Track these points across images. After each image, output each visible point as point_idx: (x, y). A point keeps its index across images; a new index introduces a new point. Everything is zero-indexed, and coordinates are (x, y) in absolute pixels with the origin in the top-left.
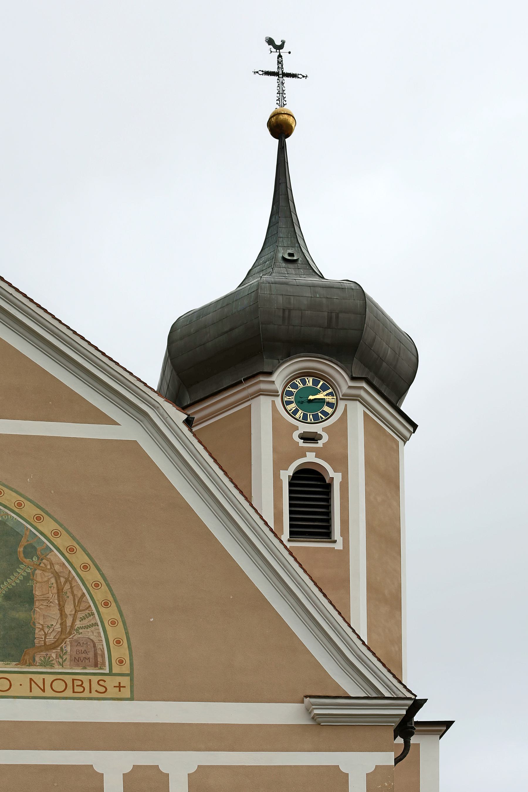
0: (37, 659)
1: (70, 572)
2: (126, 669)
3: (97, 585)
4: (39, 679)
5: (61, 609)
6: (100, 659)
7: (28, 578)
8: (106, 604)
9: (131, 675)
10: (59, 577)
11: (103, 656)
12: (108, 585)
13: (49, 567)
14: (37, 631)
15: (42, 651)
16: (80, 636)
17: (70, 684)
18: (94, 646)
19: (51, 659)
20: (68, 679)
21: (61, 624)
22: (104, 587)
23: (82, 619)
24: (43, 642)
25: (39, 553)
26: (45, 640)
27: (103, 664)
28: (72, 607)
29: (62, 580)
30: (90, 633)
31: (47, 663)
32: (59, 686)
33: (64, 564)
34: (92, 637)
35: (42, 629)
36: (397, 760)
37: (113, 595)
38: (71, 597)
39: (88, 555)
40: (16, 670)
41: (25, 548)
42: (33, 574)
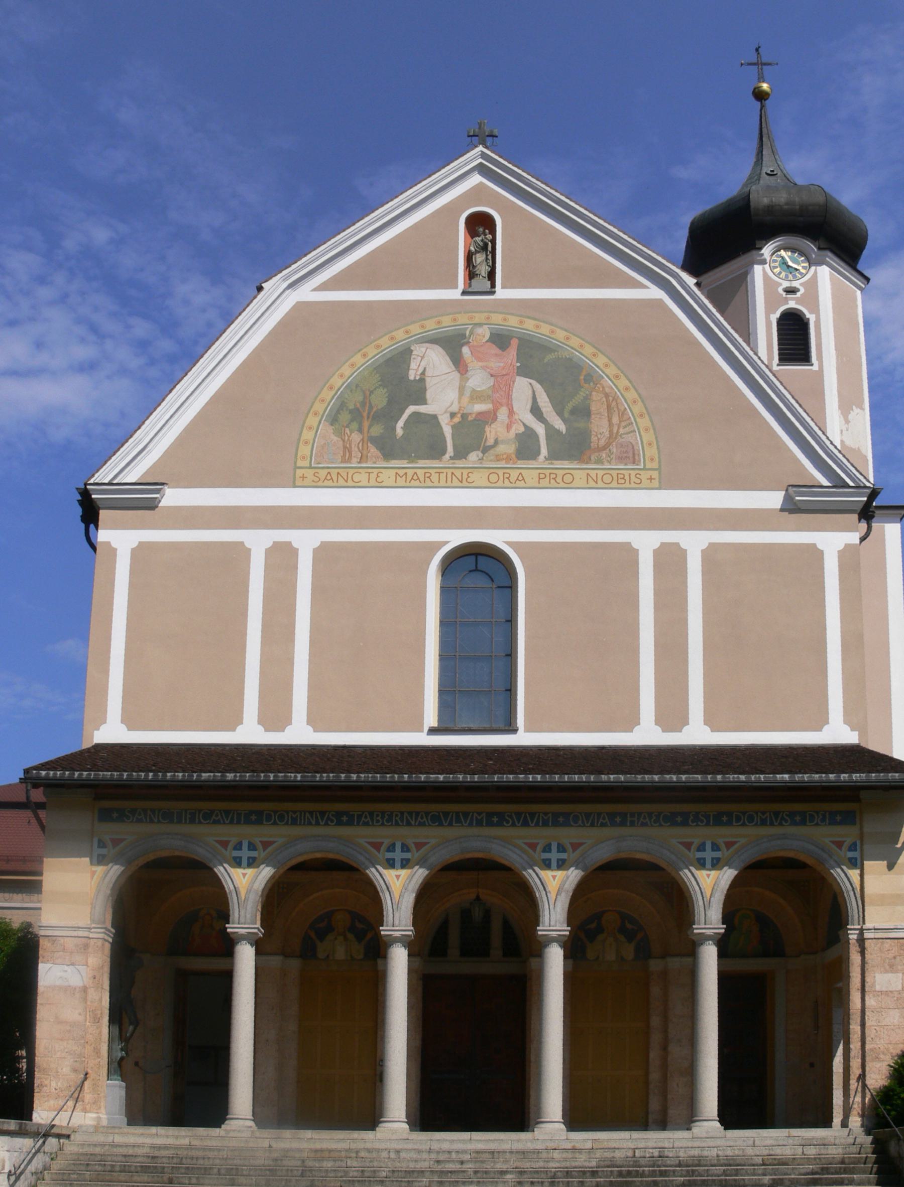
0: (592, 458)
1: (616, 393)
2: (655, 465)
3: (635, 402)
4: (593, 473)
5: (610, 420)
6: (637, 458)
7: (587, 398)
8: (641, 416)
9: (659, 469)
10: (609, 396)
11: (639, 455)
12: (643, 401)
13: (601, 389)
14: (593, 437)
15: (595, 452)
16: (623, 440)
17: (615, 477)
18: (633, 448)
19: (602, 458)
20: (614, 473)
21: (609, 431)
22: (640, 403)
23: (625, 427)
24: (596, 446)
25: (594, 379)
26: (598, 444)
27: (639, 461)
28: (618, 418)
29: (611, 399)
30: (630, 438)
31: (599, 461)
32: (607, 479)
33: (612, 388)
34: (631, 441)
35: (596, 436)
36: (863, 539)
37: (646, 408)
38: (617, 411)
39: (628, 379)
40: (578, 467)
41: (585, 376)
42: (591, 394)
